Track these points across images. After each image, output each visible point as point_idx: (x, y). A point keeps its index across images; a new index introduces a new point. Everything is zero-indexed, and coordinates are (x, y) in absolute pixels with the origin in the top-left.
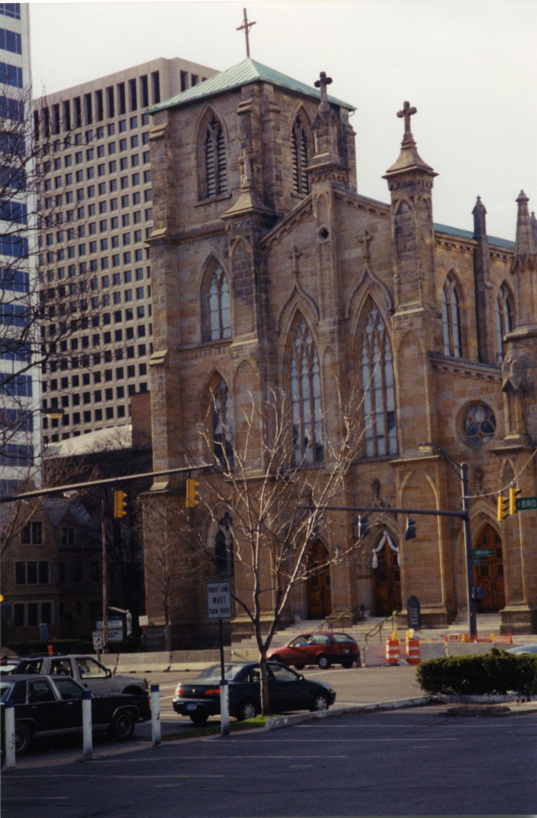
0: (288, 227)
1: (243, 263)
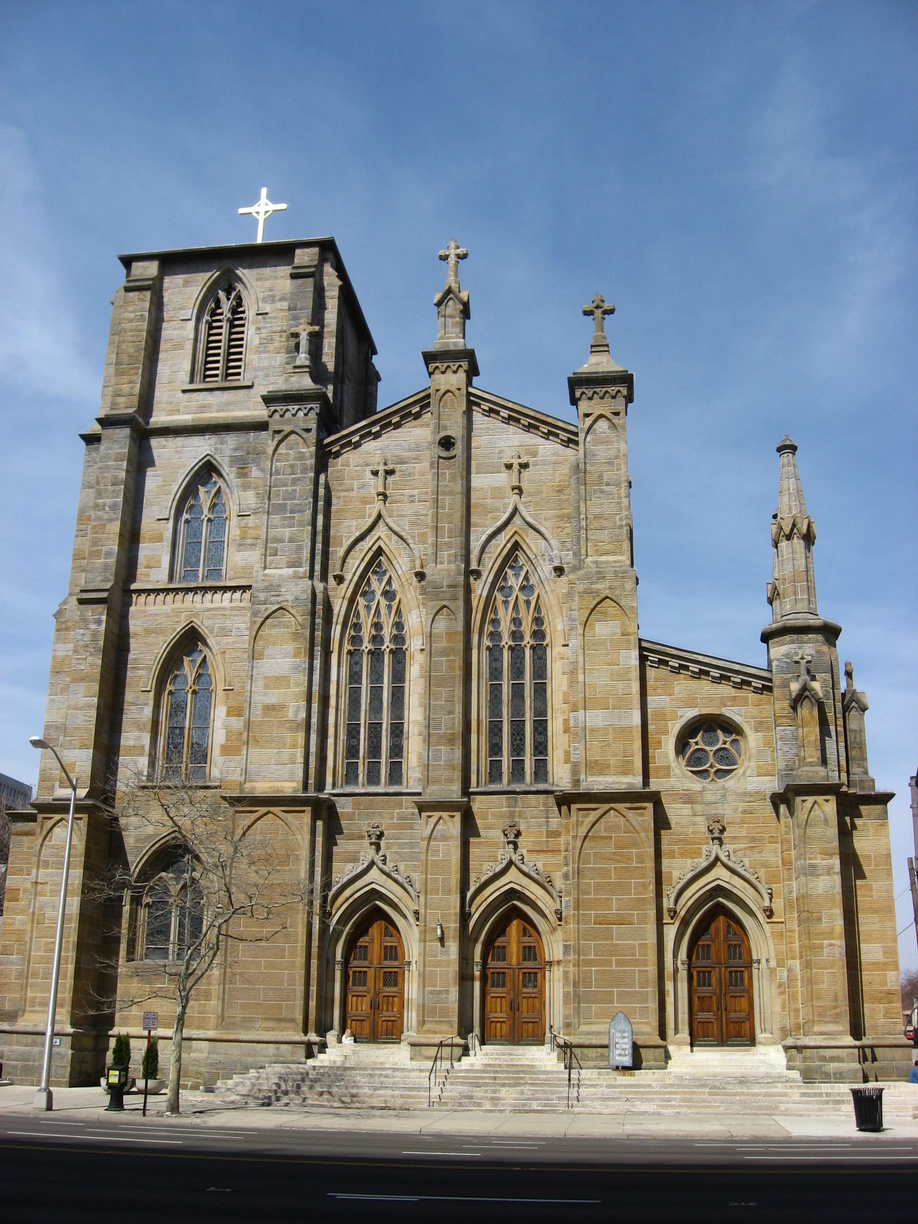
0: (375, 429)
1: (292, 466)
